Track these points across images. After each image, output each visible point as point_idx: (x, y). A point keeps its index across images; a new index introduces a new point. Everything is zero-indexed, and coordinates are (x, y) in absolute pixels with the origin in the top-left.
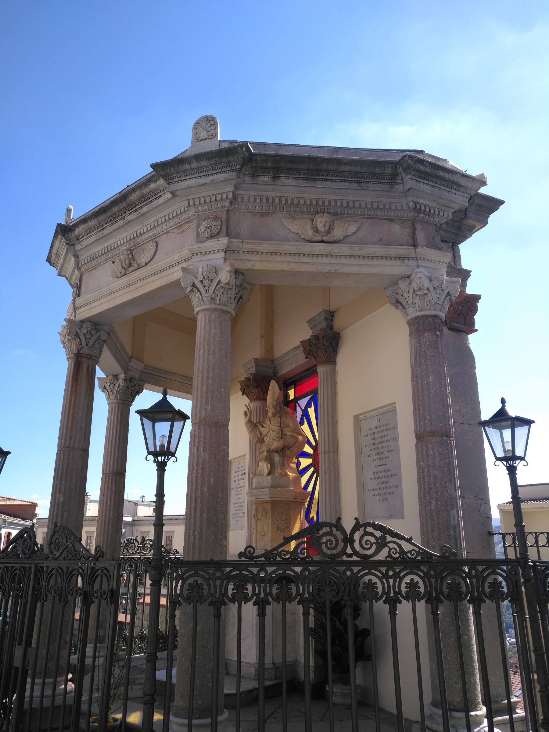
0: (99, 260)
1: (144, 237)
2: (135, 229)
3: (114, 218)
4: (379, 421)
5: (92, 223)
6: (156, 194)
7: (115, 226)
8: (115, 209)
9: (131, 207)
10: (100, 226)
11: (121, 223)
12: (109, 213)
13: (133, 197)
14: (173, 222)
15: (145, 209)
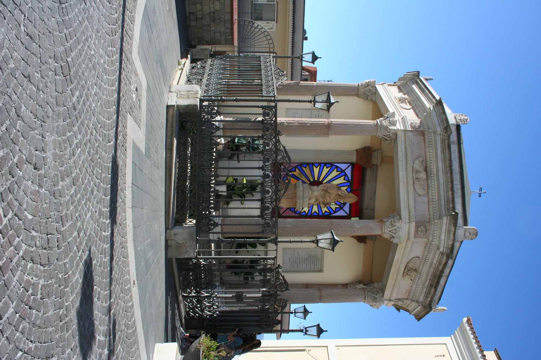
0: (426, 252)
1: (417, 279)
2: (423, 278)
3: (434, 276)
4: (319, 260)
5: (440, 268)
6: (426, 297)
7: (430, 274)
8: (436, 281)
9: (431, 286)
10: (437, 269)
11: (429, 277)
12: (437, 277)
13: (433, 291)
14: (413, 291)
15: (425, 290)
